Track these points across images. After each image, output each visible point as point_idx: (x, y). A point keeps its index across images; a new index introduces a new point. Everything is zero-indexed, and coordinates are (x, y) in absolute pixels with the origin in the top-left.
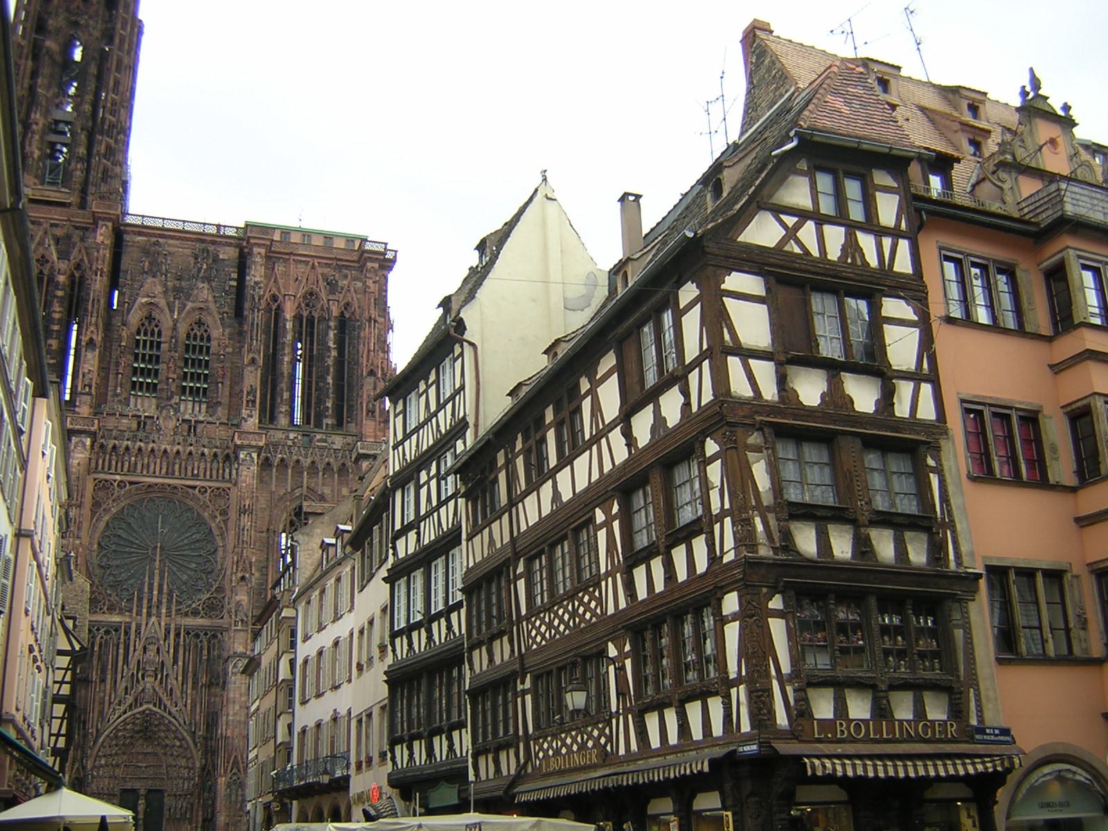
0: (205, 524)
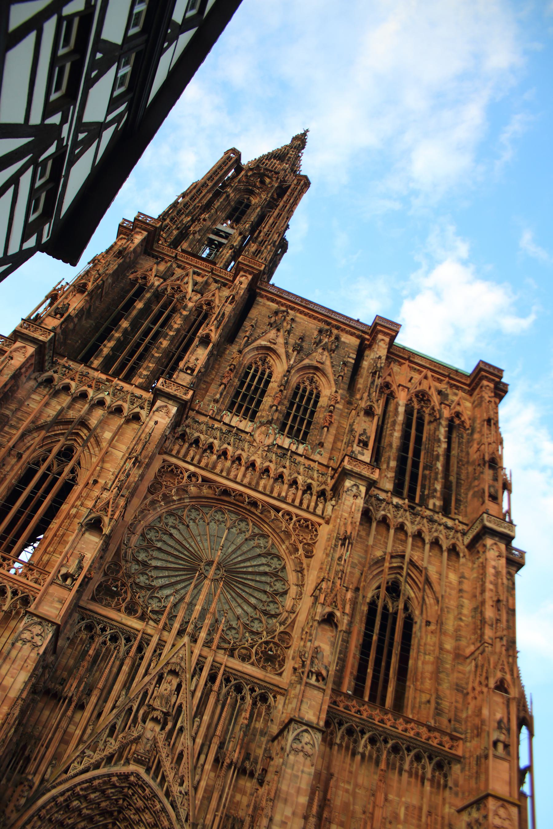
0: (279, 560)
